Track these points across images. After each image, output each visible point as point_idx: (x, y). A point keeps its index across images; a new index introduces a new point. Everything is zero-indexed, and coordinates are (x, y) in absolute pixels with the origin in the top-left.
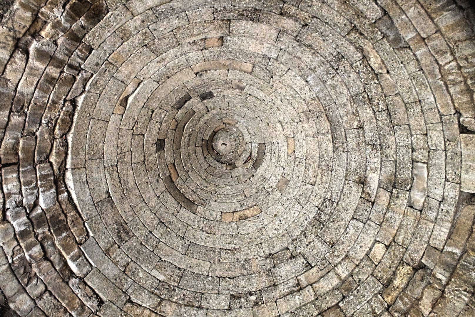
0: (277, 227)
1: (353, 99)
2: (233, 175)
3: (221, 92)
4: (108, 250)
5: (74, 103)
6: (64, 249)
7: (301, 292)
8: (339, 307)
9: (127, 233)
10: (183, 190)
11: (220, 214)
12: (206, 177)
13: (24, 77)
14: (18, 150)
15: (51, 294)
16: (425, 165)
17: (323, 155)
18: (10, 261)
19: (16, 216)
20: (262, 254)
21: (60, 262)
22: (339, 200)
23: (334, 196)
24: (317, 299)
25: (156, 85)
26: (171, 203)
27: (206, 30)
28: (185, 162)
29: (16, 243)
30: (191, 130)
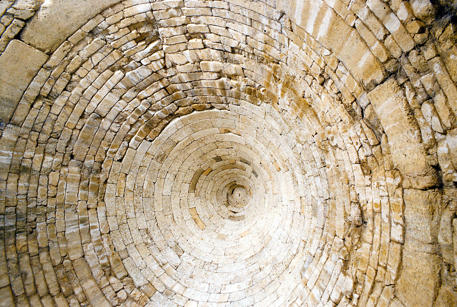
0: (195, 242)
2: (221, 207)
4: (149, 154)
5: (212, 107)
6: (139, 132)
7: (160, 267)
9: (162, 160)
12: (214, 191)
13: (208, 81)
14: (176, 92)
15: (115, 135)
18: (123, 111)
19: (144, 104)
20: (177, 239)
21: (132, 133)
23: (220, 269)
25: (244, 144)
26: (189, 178)
27: (279, 159)
28: (216, 176)
29: (132, 110)
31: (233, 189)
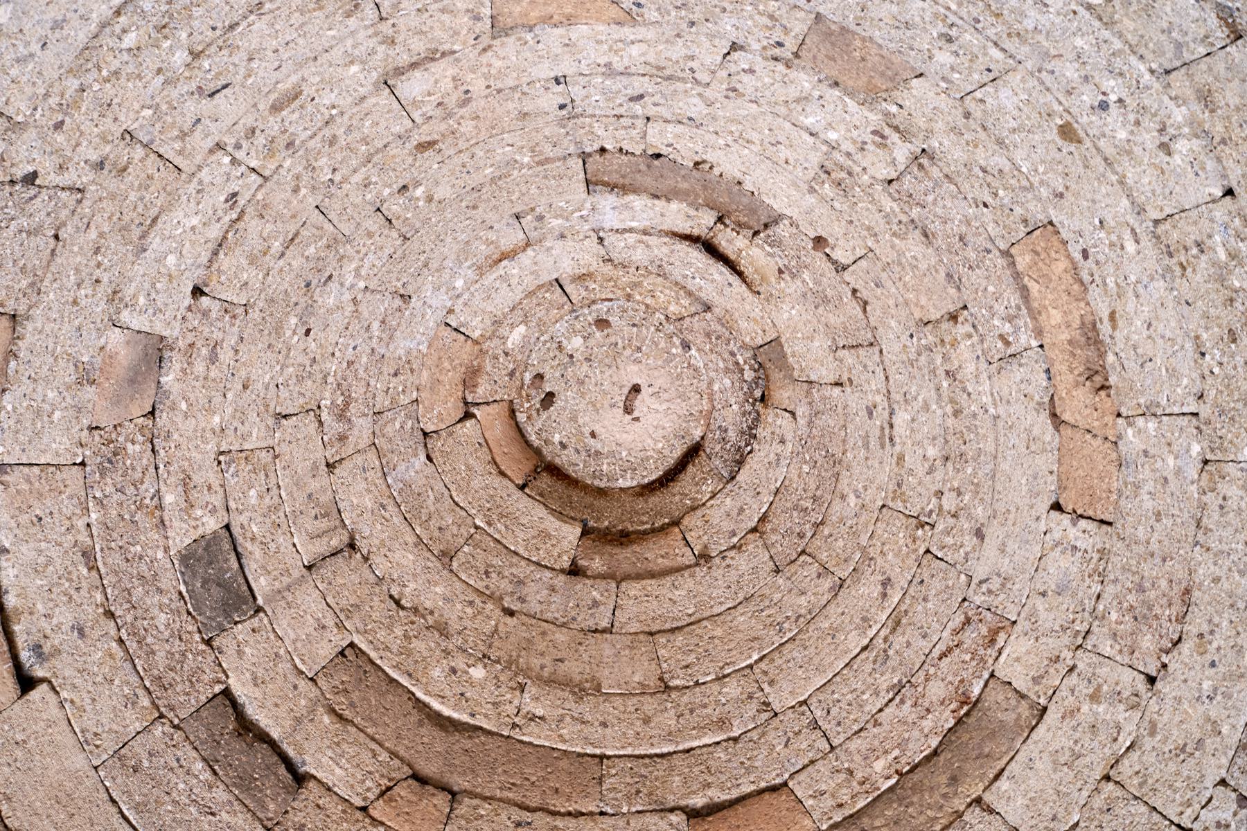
0: (1149, 138)
3: (186, 483)
10: (879, 765)
11: (1065, 520)
12: (825, 571)
28: (702, 729)
30: (478, 673)
31: (654, 500)
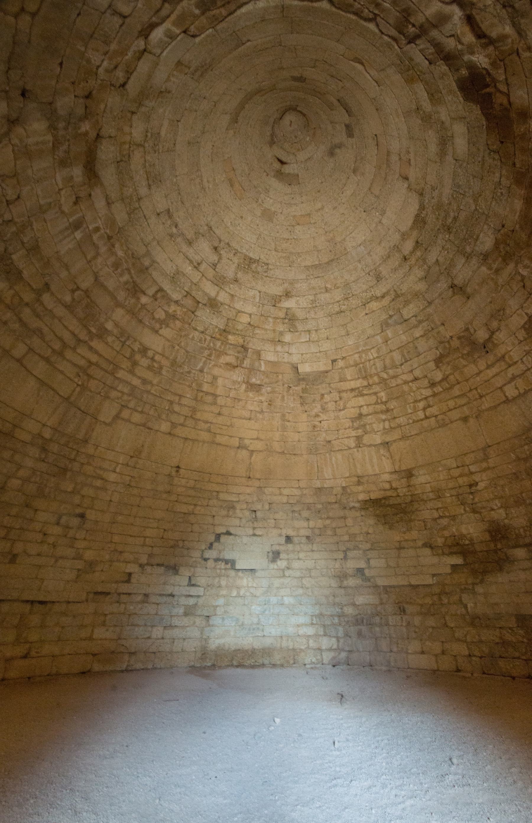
1: (347, 285)
8: (198, 305)
16: (308, 340)
17: (301, 256)
22: (270, 277)
23: (272, 272)
24: (196, 285)
